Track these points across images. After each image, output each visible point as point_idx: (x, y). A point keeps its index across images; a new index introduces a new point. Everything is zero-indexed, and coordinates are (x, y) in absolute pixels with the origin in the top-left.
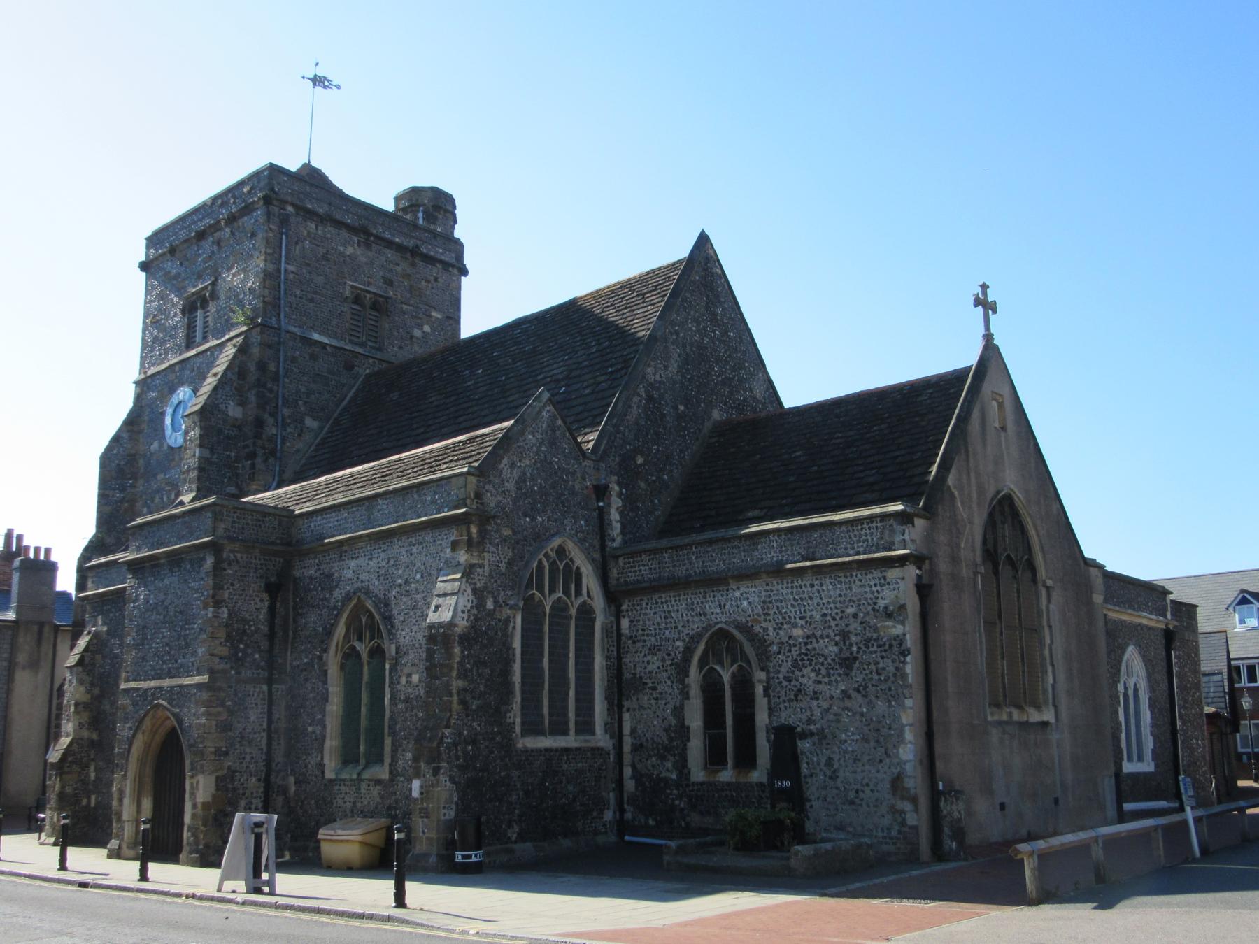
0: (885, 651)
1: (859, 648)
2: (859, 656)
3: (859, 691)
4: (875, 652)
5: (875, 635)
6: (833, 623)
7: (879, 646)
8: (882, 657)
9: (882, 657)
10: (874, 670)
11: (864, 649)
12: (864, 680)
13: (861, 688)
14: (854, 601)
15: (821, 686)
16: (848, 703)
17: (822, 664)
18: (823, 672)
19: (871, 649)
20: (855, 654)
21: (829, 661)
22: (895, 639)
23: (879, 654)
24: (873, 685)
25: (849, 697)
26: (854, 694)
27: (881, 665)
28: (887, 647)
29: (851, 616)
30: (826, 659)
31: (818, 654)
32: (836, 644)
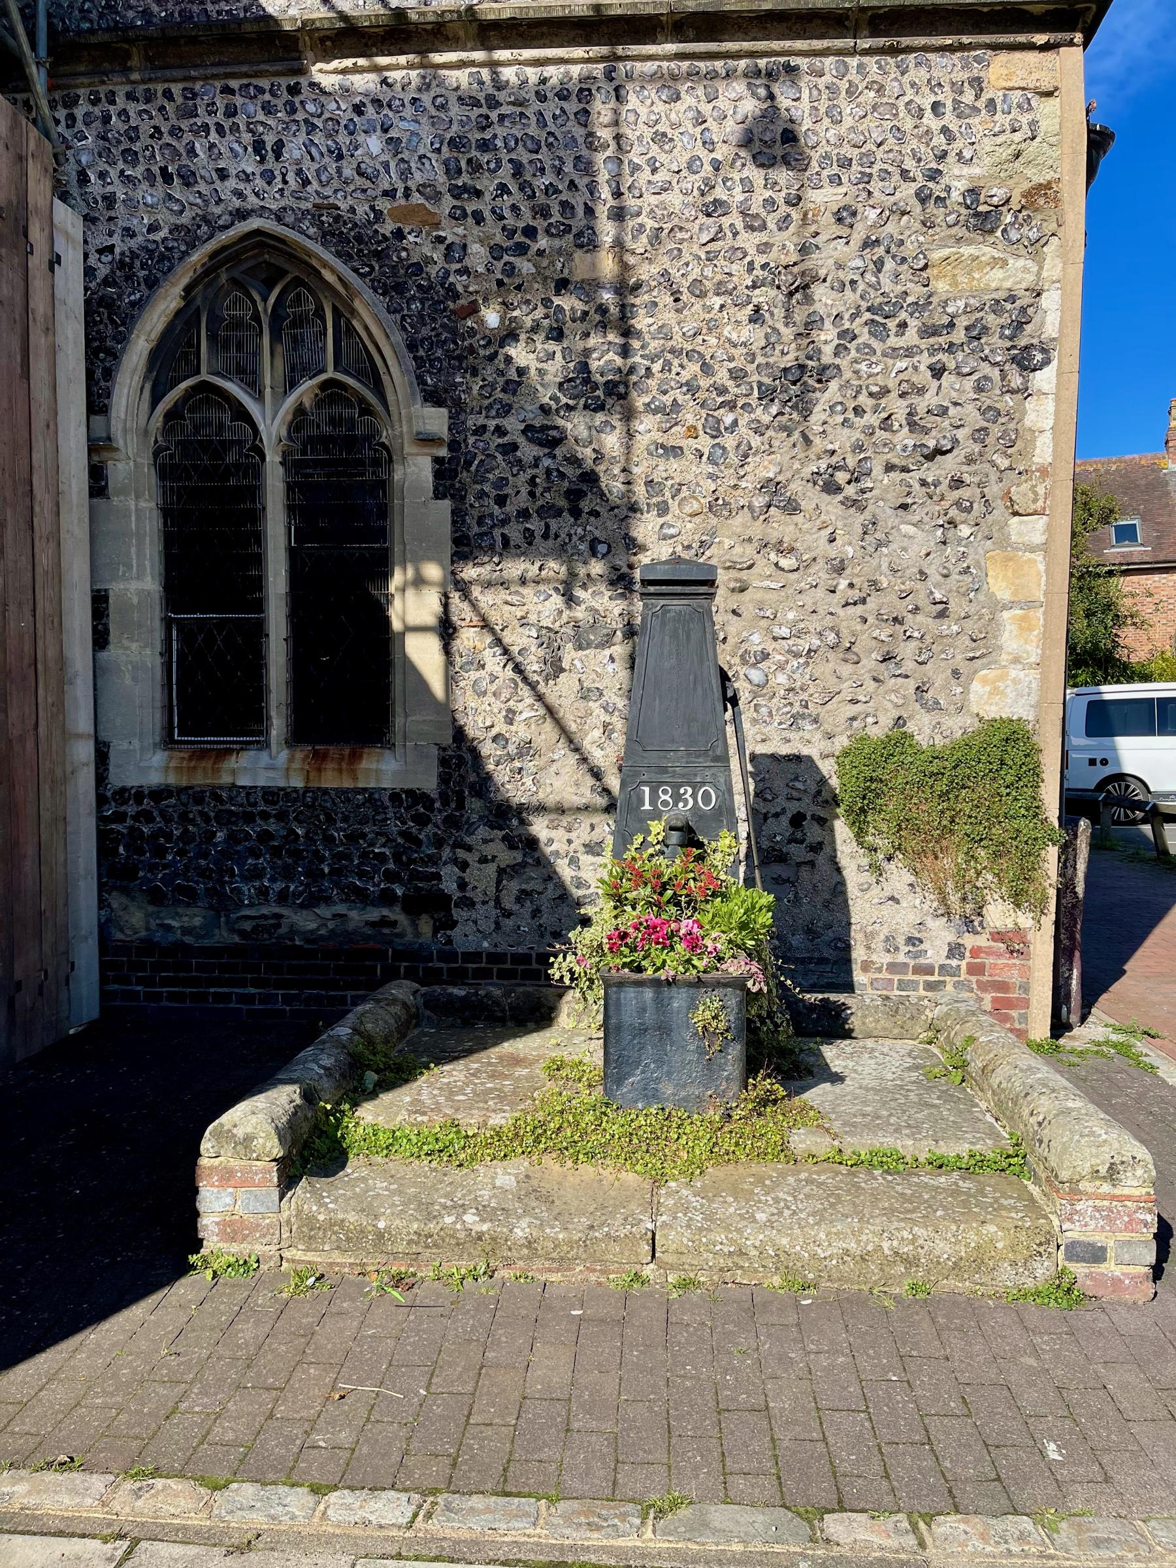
0: (951, 348)
1: (847, 335)
2: (843, 362)
3: (832, 488)
4: (909, 352)
5: (916, 291)
6: (749, 241)
7: (929, 331)
8: (938, 372)
9: (938, 372)
10: (900, 416)
11: (864, 337)
12: (859, 447)
13: (841, 477)
14: (846, 163)
15: (674, 464)
16: (781, 527)
17: (691, 388)
18: (690, 416)
19: (893, 341)
20: (827, 358)
21: (722, 376)
22: (997, 307)
23: (925, 360)
24: (890, 468)
25: (792, 507)
26: (810, 498)
27: (930, 399)
28: (959, 336)
29: (828, 219)
30: (706, 369)
31: (672, 351)
32: (757, 316)
